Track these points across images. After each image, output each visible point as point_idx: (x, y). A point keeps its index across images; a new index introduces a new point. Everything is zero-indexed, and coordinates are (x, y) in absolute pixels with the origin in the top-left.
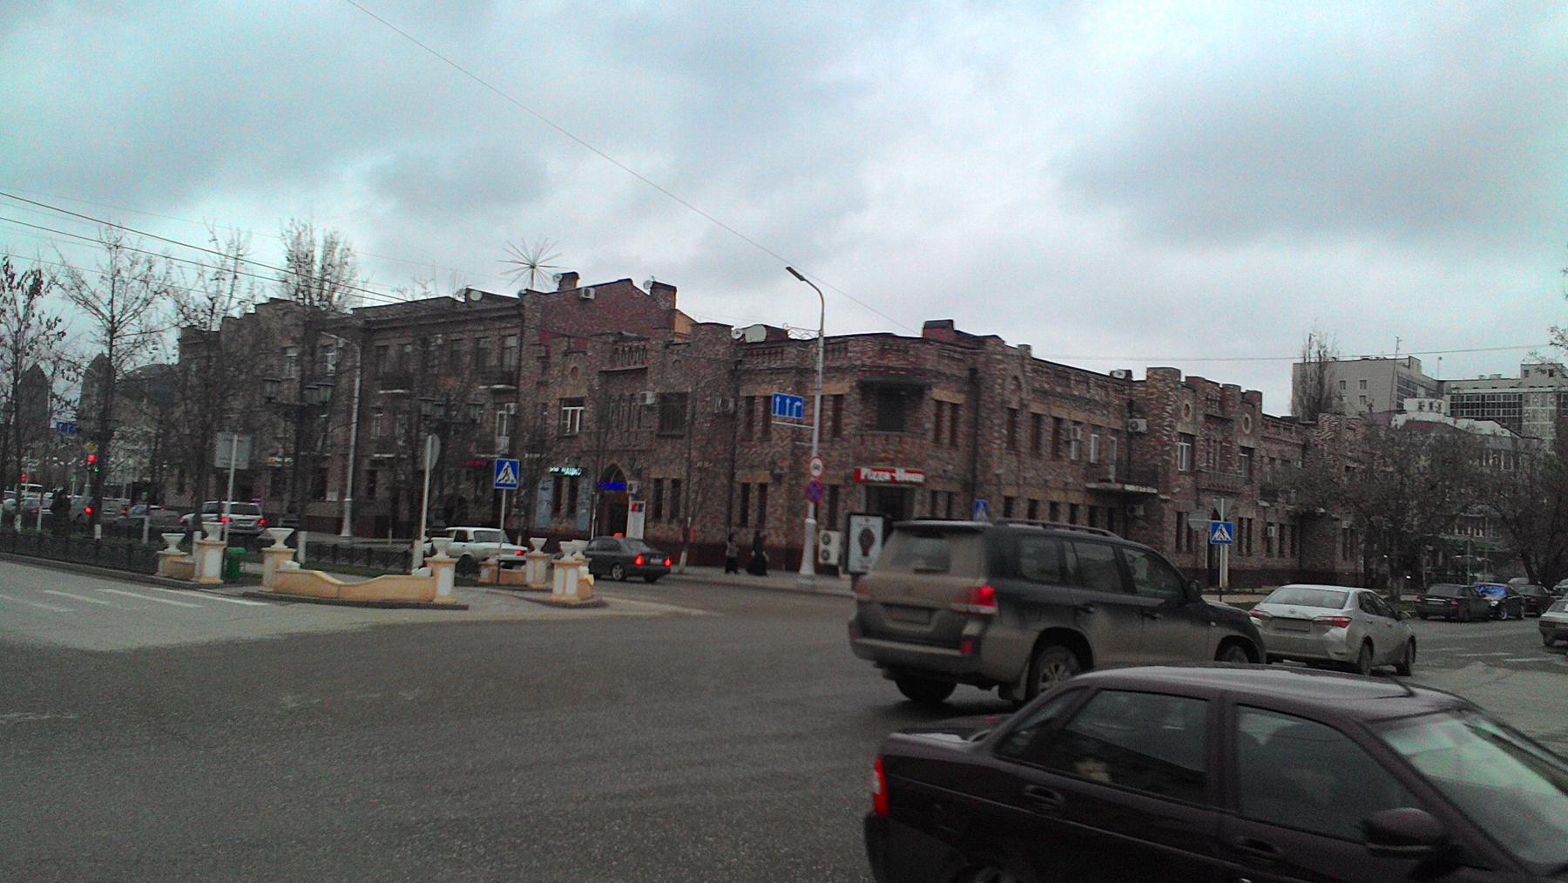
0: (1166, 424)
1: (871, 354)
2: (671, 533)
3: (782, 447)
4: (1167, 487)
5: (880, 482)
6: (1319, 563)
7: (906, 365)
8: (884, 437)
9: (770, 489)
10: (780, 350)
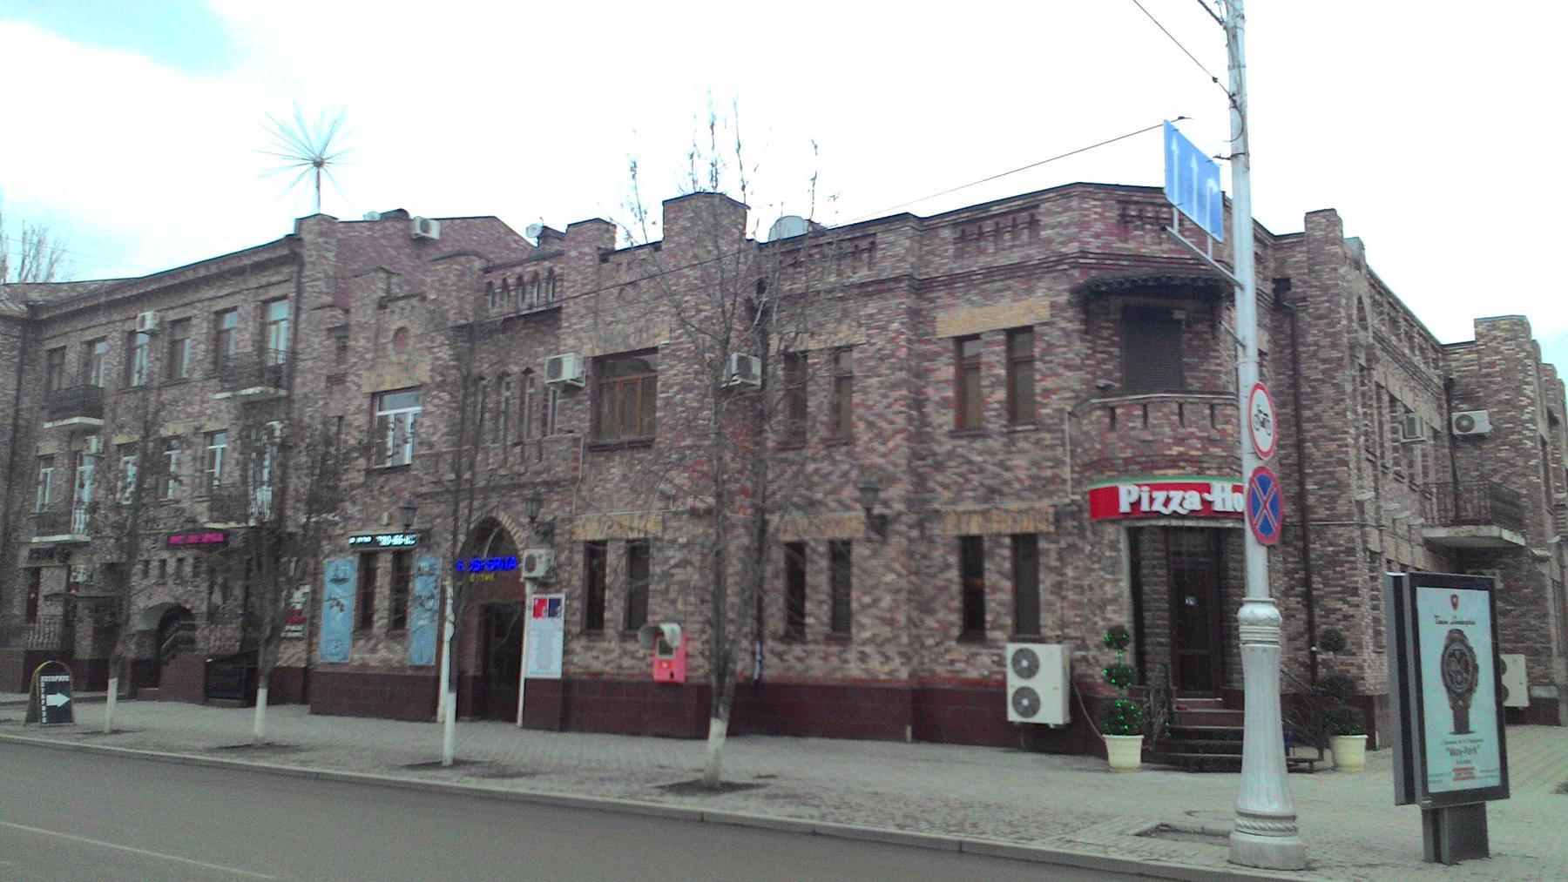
0: (1526, 417)
1: (1098, 227)
2: (627, 662)
3: (884, 455)
4: (1541, 534)
5: (1175, 515)
7: (1171, 251)
8: (1175, 407)
9: (859, 552)
10: (864, 244)
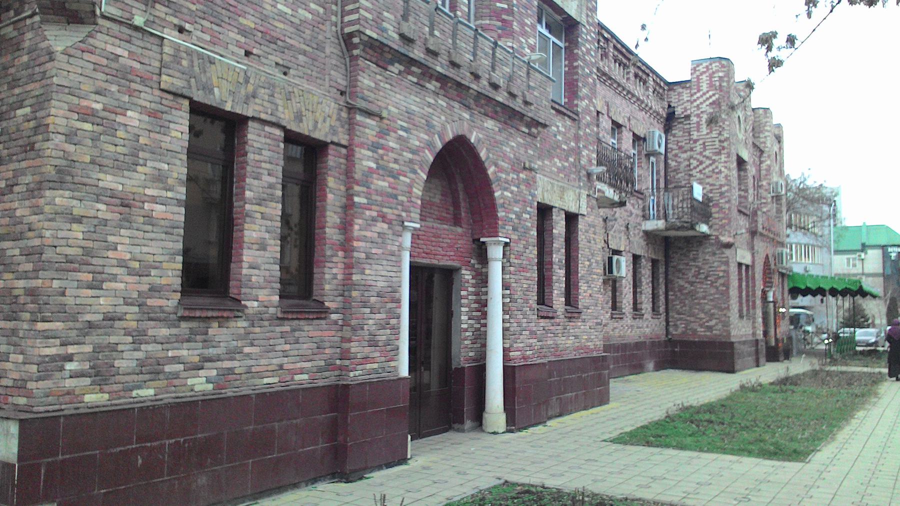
6: (701, 326)
